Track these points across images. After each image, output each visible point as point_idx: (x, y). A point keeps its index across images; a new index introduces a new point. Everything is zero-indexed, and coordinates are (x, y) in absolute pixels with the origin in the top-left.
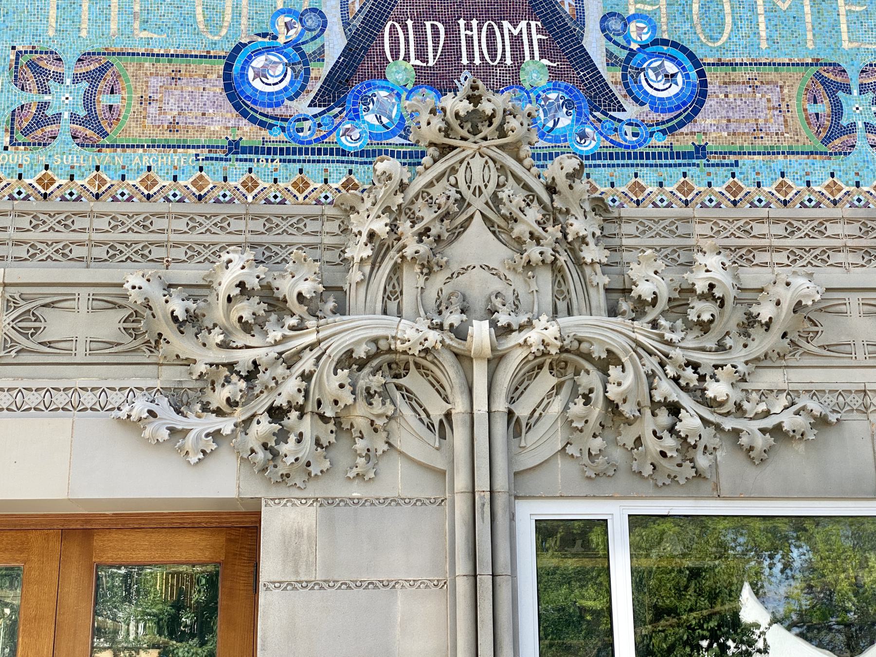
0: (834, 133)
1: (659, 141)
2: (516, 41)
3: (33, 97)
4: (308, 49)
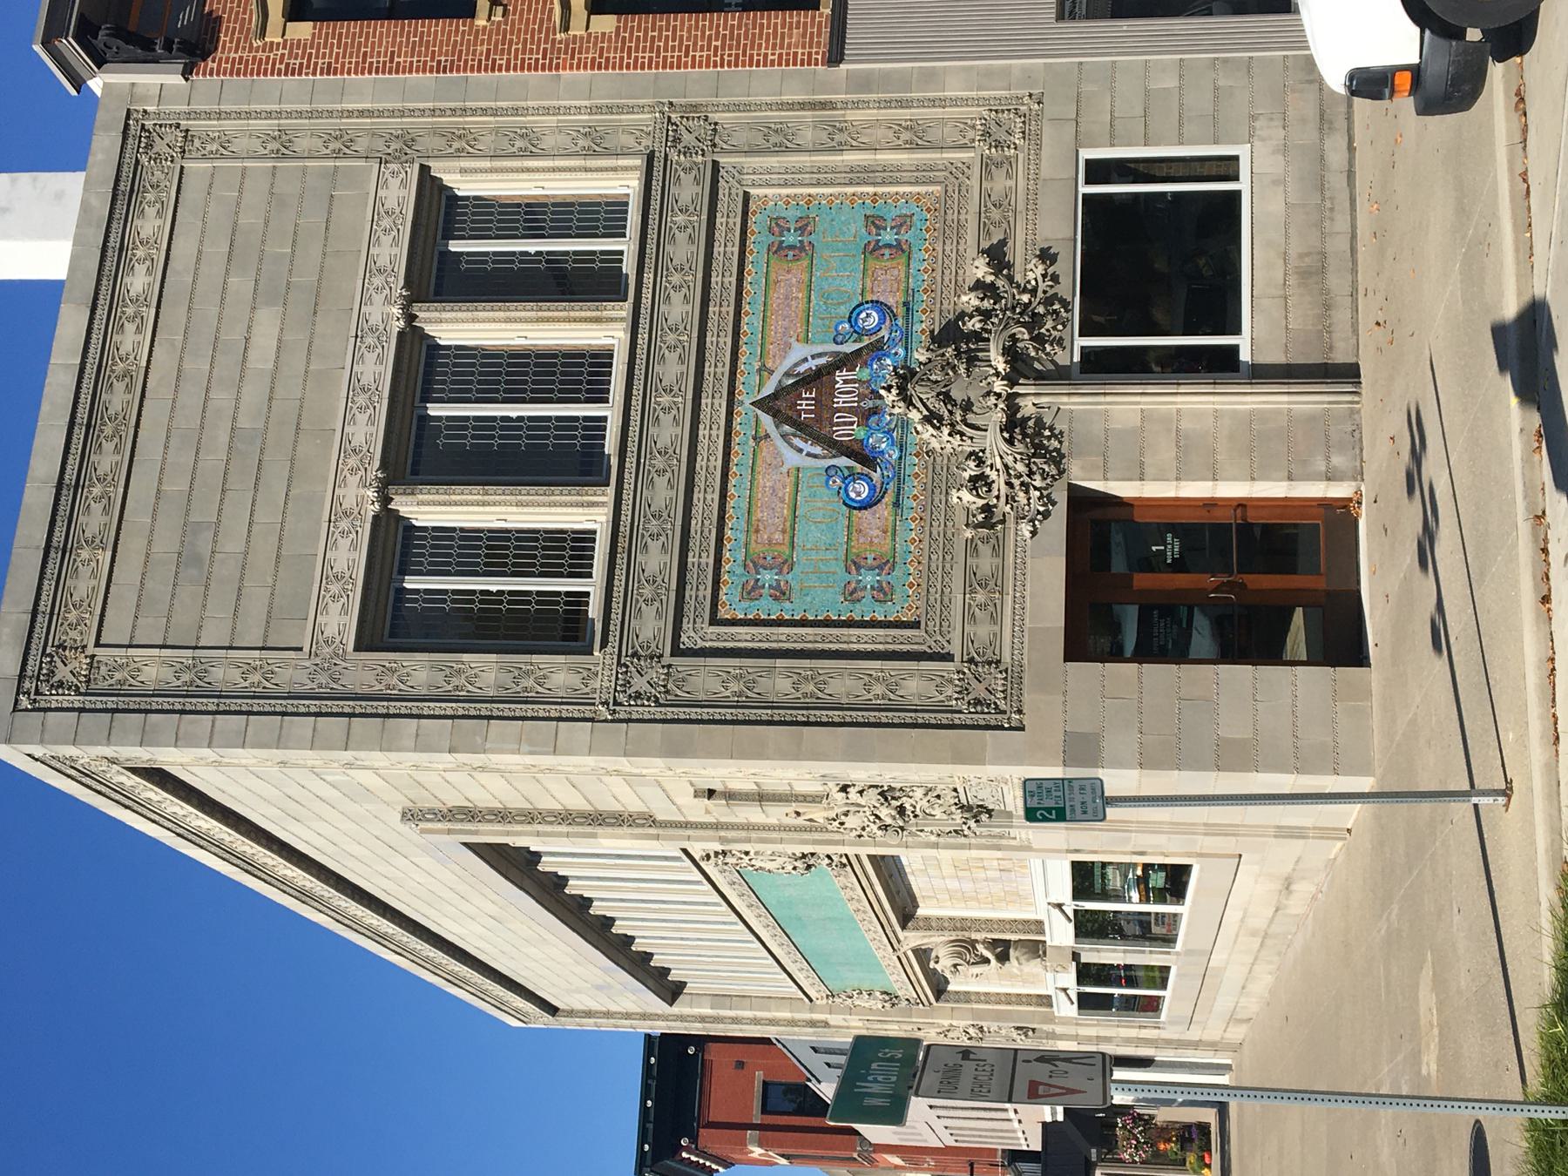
0: (898, 247)
1: (900, 322)
2: (845, 382)
3: (868, 594)
4: (846, 473)
